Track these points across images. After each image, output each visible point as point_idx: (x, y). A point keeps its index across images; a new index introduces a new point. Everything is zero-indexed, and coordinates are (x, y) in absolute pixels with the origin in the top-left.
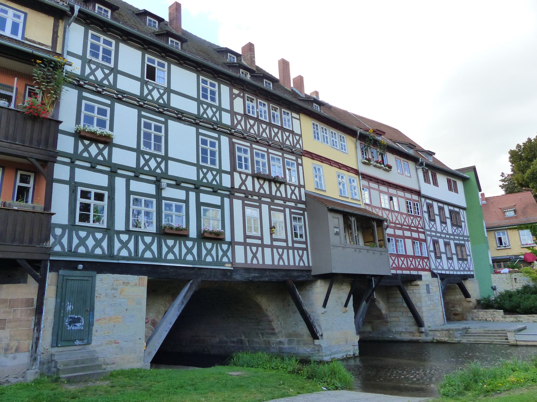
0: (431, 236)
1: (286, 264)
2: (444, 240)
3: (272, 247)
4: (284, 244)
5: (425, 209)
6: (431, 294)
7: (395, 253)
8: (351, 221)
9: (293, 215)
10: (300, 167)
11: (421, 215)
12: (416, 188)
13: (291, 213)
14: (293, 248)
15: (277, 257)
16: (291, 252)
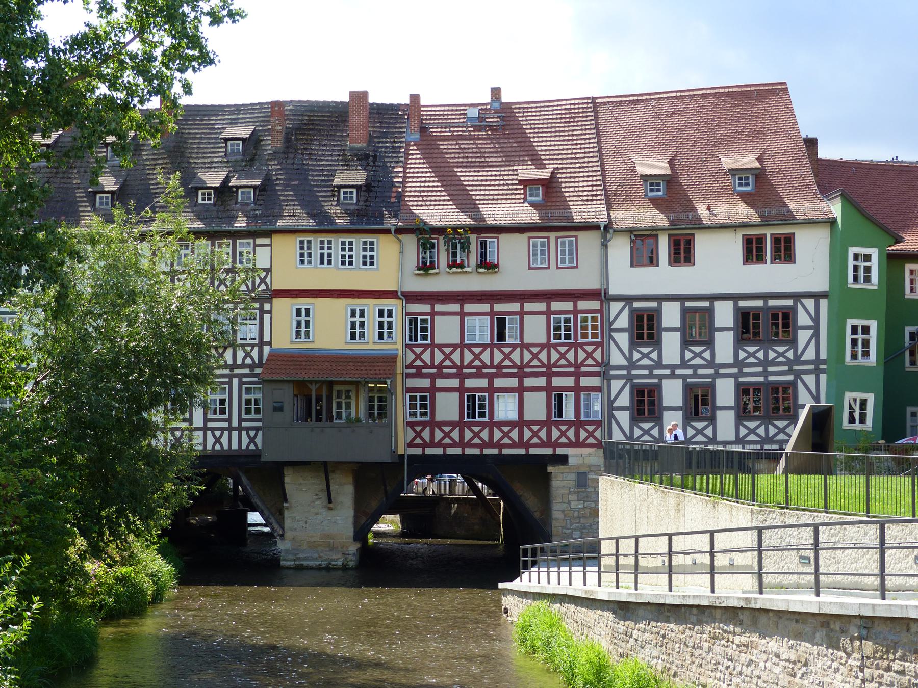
0: (629, 378)
1: (226, 448)
2: (689, 380)
3: (205, 429)
4: (226, 425)
5: (624, 321)
6: (589, 490)
7: (487, 419)
8: (311, 391)
9: (244, 386)
10: (267, 317)
11: (602, 338)
12: (592, 284)
13: (241, 383)
14: (240, 429)
15: (211, 440)
16: (235, 434)
